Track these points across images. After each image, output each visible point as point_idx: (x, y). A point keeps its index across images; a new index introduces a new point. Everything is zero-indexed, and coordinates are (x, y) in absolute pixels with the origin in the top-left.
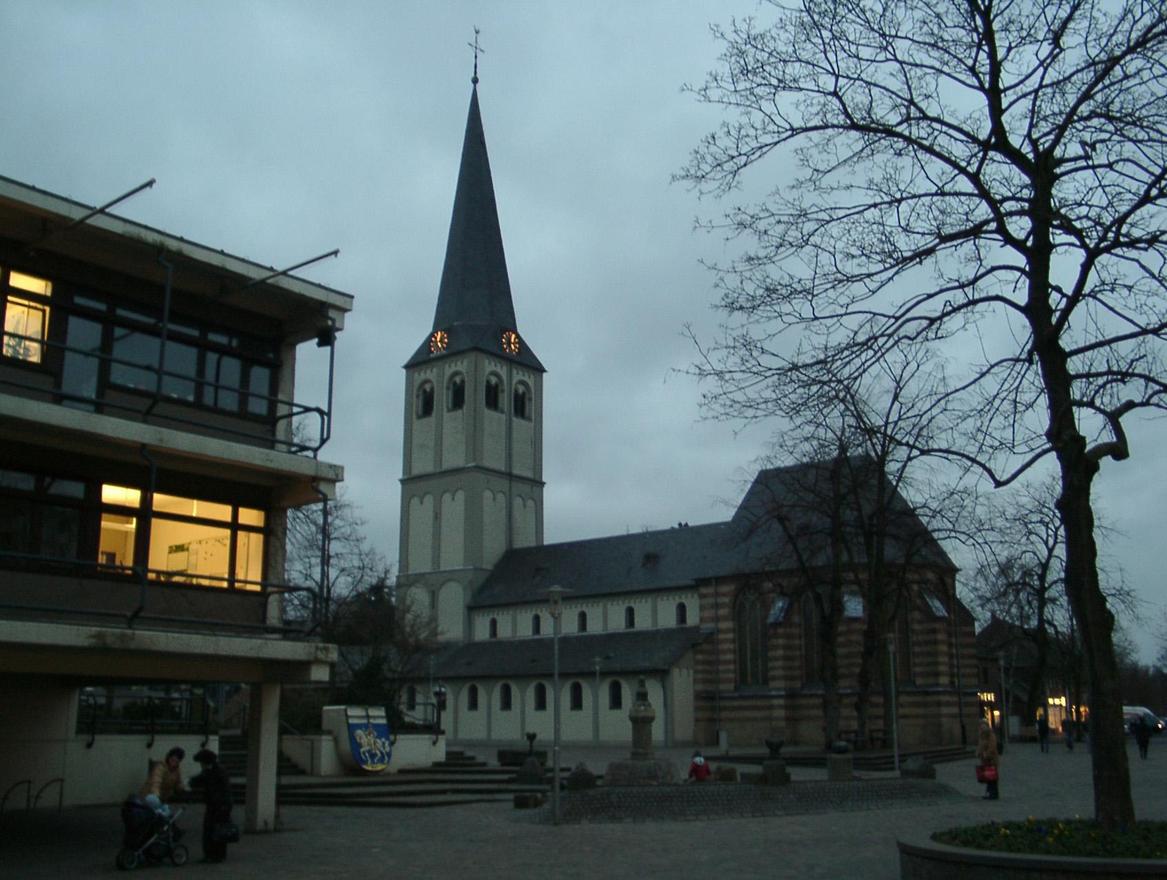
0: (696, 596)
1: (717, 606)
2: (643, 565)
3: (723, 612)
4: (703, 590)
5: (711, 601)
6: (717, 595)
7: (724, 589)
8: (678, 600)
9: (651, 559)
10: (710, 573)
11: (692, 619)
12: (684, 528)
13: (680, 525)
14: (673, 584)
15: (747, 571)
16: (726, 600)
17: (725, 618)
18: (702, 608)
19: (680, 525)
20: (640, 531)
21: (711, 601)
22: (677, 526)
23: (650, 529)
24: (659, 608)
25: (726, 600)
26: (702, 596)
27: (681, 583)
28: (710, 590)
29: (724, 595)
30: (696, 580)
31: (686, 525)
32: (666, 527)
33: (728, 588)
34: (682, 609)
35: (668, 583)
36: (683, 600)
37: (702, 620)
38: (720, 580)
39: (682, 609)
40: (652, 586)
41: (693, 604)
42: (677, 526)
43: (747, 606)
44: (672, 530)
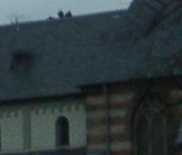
1: (110, 121)
2: (12, 67)
3: (117, 129)
4: (92, 100)
5: (101, 114)
6: (109, 106)
7: (120, 98)
8: (57, 113)
9: (22, 59)
10: (101, 78)
11: (77, 138)
12: (65, 18)
13: (61, 14)
14: (52, 92)
15: (149, 75)
16: (121, 113)
17: (121, 138)
18: (90, 124)
19: (61, 14)
20: (7, 22)
21: (101, 114)
22: (56, 16)
23: (20, 21)
24: (32, 124)
25: (121, 113)
26: (89, 108)
27: (62, 90)
28: (100, 100)
29: (118, 106)
30: (82, 87)
31: (69, 14)
32: (43, 17)
33: (124, 98)
34: (63, 125)
35: (44, 92)
36: (65, 114)
37: (89, 139)
38: (113, 87)
39: (63, 125)
40: (23, 95)
42: (56, 16)
44: (51, 21)
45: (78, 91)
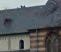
0: (28, 37)
1: (38, 41)
2: (4, 24)
3: (41, 44)
4: (32, 34)
6: (38, 36)
9: (8, 21)
10: (35, 27)
11: (26, 47)
12: (23, 8)
13: (22, 6)
15: (52, 26)
17: (42, 46)
18: (31, 42)
19: (22, 6)
20: (3, 9)
21: (35, 39)
23: (7, 9)
25: (42, 39)
26: (31, 37)
28: (35, 34)
29: (41, 36)
30: (29, 30)
32: (16, 7)
33: (44, 34)
34: (22, 42)
35: (16, 32)
37: (31, 47)
38: (39, 30)
39: (22, 42)
40: (8, 33)
41: (27, 41)
43: (52, 41)
44: (18, 9)
45: (27, 31)
